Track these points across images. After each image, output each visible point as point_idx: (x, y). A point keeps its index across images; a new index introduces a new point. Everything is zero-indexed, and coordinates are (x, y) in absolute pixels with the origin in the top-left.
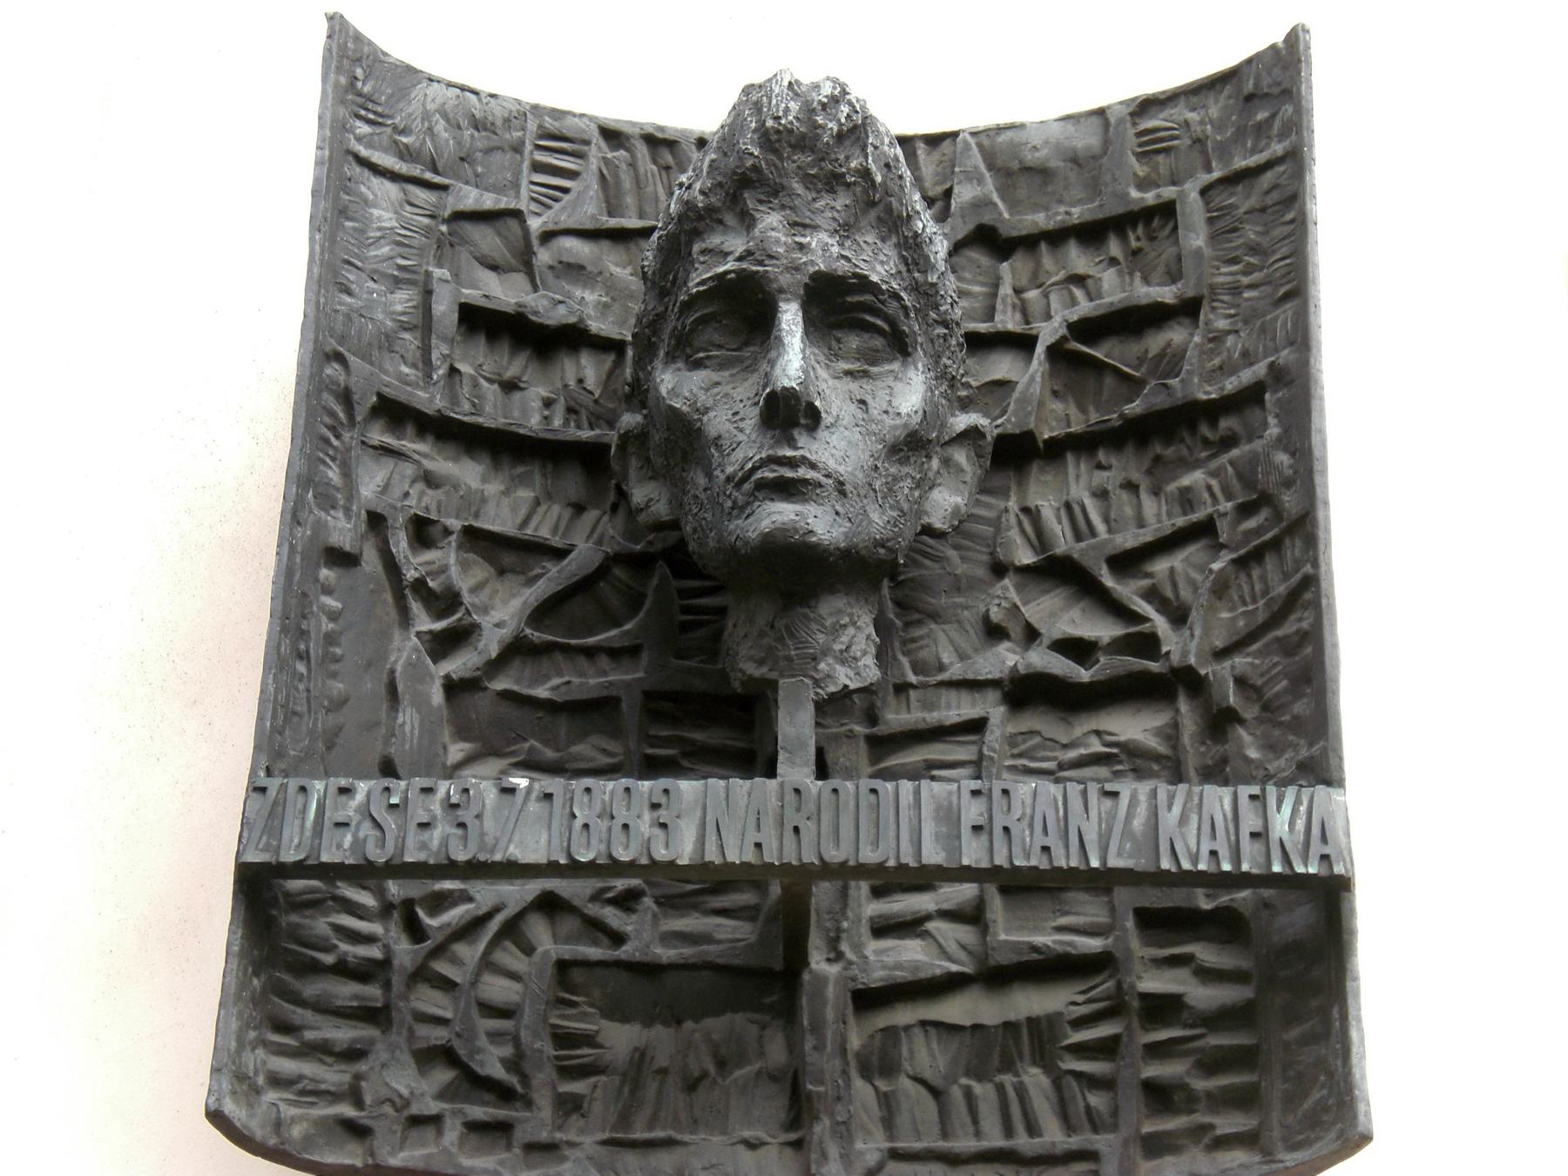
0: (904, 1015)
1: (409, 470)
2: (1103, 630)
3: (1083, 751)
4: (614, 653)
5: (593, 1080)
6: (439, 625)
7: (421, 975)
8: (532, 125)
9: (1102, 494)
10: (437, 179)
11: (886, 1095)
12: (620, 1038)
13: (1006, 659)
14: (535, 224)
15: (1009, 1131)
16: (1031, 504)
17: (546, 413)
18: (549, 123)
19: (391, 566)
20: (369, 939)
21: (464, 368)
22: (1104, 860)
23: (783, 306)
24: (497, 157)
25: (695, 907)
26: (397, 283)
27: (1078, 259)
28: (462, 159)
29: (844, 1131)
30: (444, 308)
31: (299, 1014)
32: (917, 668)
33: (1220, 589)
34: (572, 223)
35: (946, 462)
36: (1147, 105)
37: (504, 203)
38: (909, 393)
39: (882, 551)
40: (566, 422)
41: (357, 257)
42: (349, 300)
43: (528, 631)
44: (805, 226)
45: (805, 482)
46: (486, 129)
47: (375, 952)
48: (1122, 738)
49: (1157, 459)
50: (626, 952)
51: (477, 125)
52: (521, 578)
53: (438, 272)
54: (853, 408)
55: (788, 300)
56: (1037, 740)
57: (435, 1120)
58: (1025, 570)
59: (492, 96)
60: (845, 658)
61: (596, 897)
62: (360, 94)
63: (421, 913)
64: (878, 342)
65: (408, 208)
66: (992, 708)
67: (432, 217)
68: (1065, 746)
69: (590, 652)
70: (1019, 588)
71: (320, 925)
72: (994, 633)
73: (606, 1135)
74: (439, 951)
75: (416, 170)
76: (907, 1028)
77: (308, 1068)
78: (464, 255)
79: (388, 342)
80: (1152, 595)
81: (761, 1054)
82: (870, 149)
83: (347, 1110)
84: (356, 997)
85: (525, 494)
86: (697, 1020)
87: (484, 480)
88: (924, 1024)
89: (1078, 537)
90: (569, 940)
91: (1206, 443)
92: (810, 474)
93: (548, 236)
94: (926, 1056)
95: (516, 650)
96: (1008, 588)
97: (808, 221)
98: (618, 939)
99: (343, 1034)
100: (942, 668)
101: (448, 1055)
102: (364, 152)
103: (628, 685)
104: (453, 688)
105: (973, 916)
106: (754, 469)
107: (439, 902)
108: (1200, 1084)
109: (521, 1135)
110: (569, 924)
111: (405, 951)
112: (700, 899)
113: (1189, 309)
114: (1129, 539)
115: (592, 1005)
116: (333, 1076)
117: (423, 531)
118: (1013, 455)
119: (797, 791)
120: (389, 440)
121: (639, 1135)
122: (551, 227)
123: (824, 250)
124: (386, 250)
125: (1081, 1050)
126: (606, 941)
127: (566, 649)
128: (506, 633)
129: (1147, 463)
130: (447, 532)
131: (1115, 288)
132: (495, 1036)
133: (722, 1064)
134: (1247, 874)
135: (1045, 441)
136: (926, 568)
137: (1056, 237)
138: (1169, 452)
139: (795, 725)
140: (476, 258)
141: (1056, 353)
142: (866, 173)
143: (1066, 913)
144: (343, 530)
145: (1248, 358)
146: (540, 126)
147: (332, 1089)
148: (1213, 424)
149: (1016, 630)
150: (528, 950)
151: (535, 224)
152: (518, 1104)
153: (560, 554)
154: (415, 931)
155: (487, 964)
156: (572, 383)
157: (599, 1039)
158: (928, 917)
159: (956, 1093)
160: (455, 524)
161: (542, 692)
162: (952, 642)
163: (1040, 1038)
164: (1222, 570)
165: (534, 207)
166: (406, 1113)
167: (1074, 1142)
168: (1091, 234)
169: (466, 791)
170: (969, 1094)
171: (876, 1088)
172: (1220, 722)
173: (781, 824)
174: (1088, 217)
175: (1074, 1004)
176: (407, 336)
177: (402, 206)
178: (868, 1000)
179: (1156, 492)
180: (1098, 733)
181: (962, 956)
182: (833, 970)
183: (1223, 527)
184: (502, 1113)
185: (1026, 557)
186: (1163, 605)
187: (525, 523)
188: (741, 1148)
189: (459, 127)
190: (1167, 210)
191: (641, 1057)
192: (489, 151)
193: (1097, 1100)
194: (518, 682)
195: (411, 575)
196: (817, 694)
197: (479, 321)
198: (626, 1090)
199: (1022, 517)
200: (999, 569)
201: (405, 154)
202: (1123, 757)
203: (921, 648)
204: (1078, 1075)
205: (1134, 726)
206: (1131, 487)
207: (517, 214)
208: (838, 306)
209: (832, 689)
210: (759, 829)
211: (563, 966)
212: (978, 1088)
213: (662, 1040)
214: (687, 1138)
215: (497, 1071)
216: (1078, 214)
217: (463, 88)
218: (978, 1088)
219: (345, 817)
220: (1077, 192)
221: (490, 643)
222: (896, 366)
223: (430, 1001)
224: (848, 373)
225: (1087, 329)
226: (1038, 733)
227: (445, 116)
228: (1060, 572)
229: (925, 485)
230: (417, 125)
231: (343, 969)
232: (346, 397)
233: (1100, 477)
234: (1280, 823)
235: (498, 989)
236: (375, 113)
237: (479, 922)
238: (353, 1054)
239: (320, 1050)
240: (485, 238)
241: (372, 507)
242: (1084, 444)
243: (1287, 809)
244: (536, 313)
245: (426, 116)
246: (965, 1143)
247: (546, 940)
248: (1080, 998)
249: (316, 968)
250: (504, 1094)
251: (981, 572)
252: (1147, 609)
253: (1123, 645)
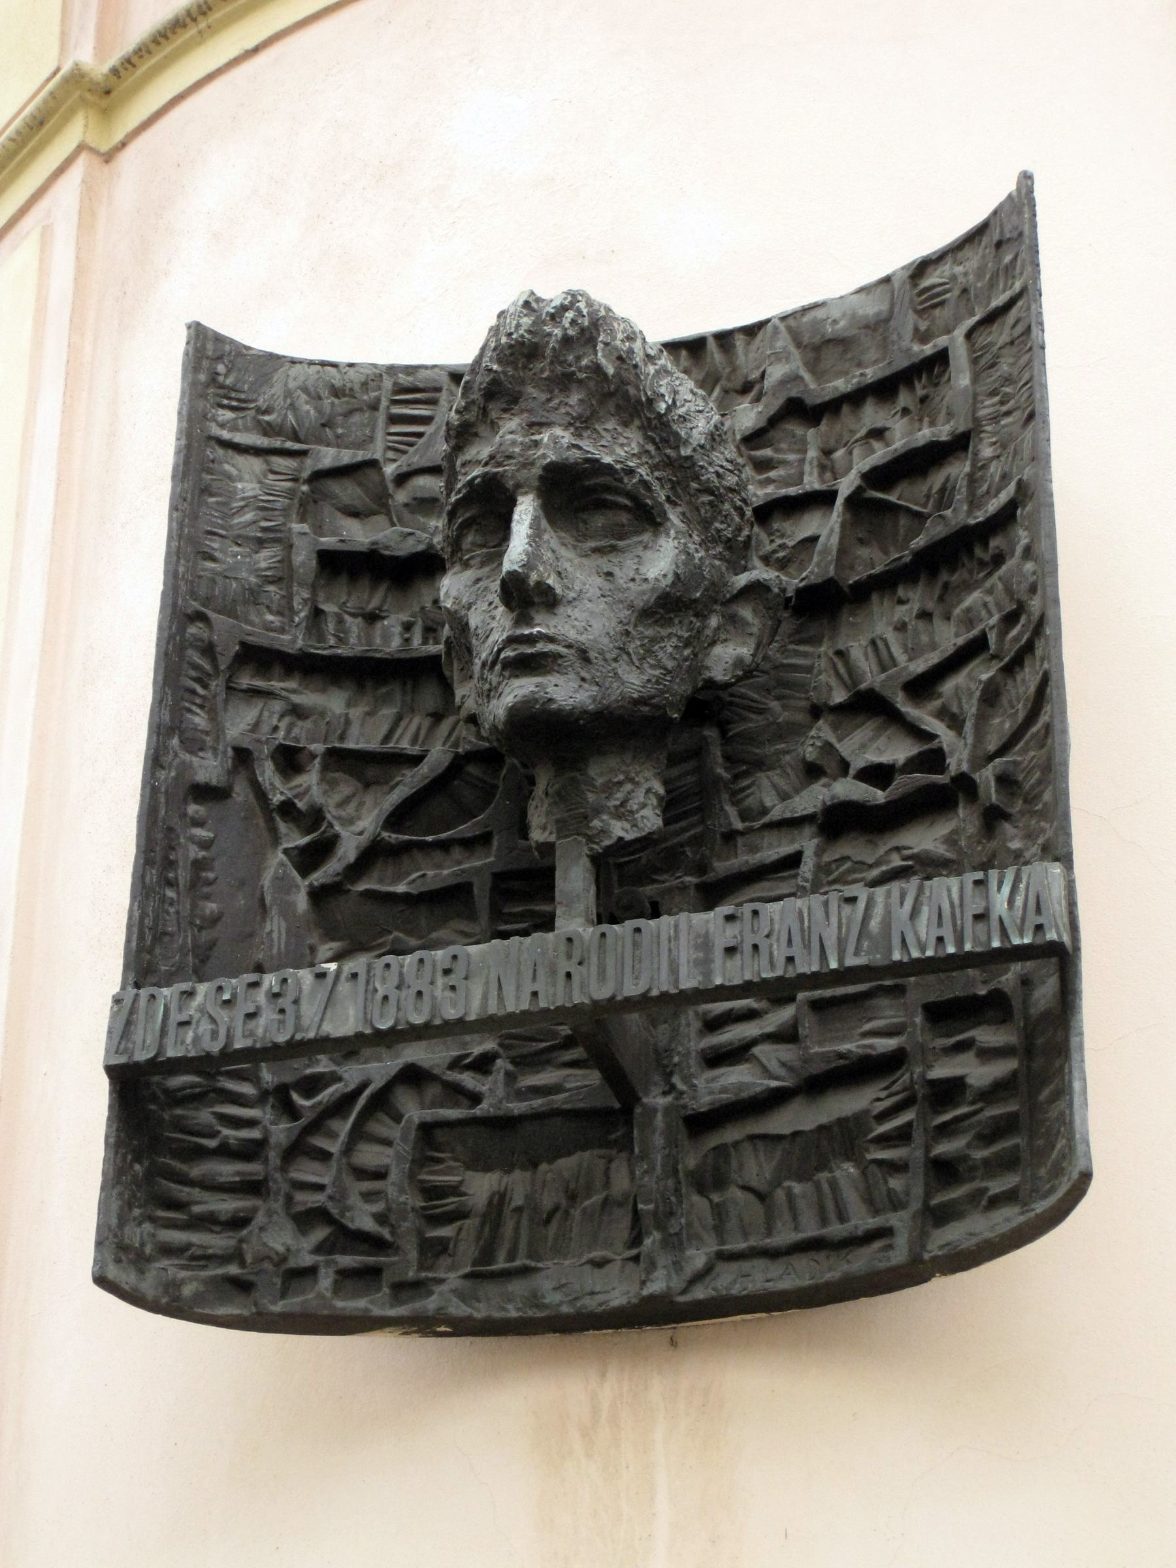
0: (731, 1134)
1: (277, 706)
3: (884, 868)
4: (468, 844)
5: (459, 1223)
6: (304, 840)
7: (296, 1150)
8: (388, 384)
9: (901, 627)
10: (297, 446)
11: (717, 1205)
12: (481, 1187)
14: (389, 470)
15: (824, 1221)
16: (841, 646)
17: (407, 636)
18: (403, 379)
19: (261, 795)
20: (251, 1123)
21: (329, 608)
22: (841, 960)
23: (520, 499)
24: (356, 418)
25: (548, 1062)
26: (260, 543)
27: (872, 415)
28: (324, 425)
30: (303, 558)
31: (183, 1192)
32: (744, 816)
34: (425, 463)
35: (733, 620)
36: (922, 267)
37: (361, 456)
38: (660, 560)
39: (646, 709)
40: (425, 642)
41: (222, 527)
42: (210, 565)
43: (385, 834)
44: (541, 425)
45: (544, 655)
46: (344, 395)
47: (255, 1134)
48: (916, 851)
49: (946, 586)
50: (484, 1108)
51: (336, 392)
52: (386, 788)
53: (297, 527)
54: (599, 581)
55: (526, 493)
56: (848, 865)
57: (310, 1272)
58: (840, 709)
59: (351, 365)
60: (622, 812)
61: (456, 1064)
62: (222, 387)
63: (295, 1096)
64: (624, 518)
65: (271, 476)
66: (807, 843)
67: (295, 480)
68: (871, 866)
69: (444, 846)
70: (835, 727)
71: (204, 1116)
72: (813, 772)
73: (468, 1270)
74: (316, 1126)
75: (277, 443)
76: (736, 1144)
77: (196, 1238)
78: (327, 510)
79: (253, 596)
80: (943, 714)
81: (607, 1184)
82: (600, 346)
83: (233, 1270)
84: (238, 1173)
85: (388, 712)
86: (551, 1161)
87: (349, 705)
88: (752, 1138)
89: (884, 669)
90: (433, 1105)
91: (982, 564)
92: (551, 647)
93: (402, 479)
94: (756, 1168)
95: (373, 854)
96: (823, 730)
97: (544, 420)
98: (475, 1098)
99: (227, 1205)
100: (765, 811)
101: (320, 1215)
102: (225, 435)
103: (478, 871)
104: (318, 896)
105: (787, 1036)
106: (500, 651)
107: (311, 1085)
108: (979, 1154)
109: (388, 1277)
110: (433, 1091)
111: (281, 1131)
112: (555, 1054)
114: (919, 666)
115: (456, 1160)
116: (217, 1242)
117: (290, 760)
118: (822, 605)
119: (570, 940)
120: (259, 683)
121: (501, 1264)
122: (405, 469)
123: (557, 442)
124: (249, 516)
125: (884, 1140)
126: (465, 1102)
127: (422, 846)
128: (364, 840)
129: (937, 592)
130: (313, 756)
131: (905, 434)
132: (368, 1197)
133: (573, 1197)
134: (970, 954)
135: (851, 587)
136: (751, 720)
137: (856, 398)
138: (955, 578)
139: (575, 880)
140: (339, 510)
141: (855, 502)
142: (597, 369)
143: (870, 1020)
144: (209, 768)
146: (395, 384)
147: (219, 1252)
148: (986, 545)
149: (831, 766)
150: (397, 1118)
151: (389, 470)
152: (390, 1251)
153: (417, 760)
154: (292, 1112)
155: (358, 1134)
156: (428, 605)
157: (463, 1189)
158: (754, 1042)
159: (780, 1194)
160: (318, 748)
161: (401, 888)
162: (774, 786)
163: (846, 1137)
164: (991, 679)
165: (391, 455)
166: (284, 1267)
167: (872, 1223)
169: (285, 980)
170: (790, 1196)
171: (710, 1201)
173: (553, 972)
174: (880, 375)
175: (879, 1100)
176: (271, 588)
177: (265, 476)
178: (700, 1123)
180: (897, 849)
181: (782, 1072)
182: (662, 1101)
183: (992, 638)
184: (371, 1260)
185: (839, 696)
187: (387, 738)
188: (588, 1267)
189: (320, 398)
190: (941, 358)
191: (499, 1201)
192: (349, 413)
194: (381, 881)
195: (277, 799)
196: (591, 849)
197: (336, 565)
198: (487, 1229)
199: (836, 660)
200: (816, 712)
201: (268, 430)
202: (917, 867)
203: (748, 796)
204: (880, 1163)
205: (925, 838)
207: (373, 464)
208: (575, 495)
209: (607, 843)
210: (534, 978)
211: (427, 1130)
213: (518, 1183)
214: (540, 1265)
215: (366, 1223)
216: (871, 374)
217: (323, 364)
218: (797, 1188)
219: (204, 1017)
220: (872, 355)
221: (348, 849)
222: (646, 537)
223: (308, 1172)
224: (595, 550)
226: (847, 858)
227: (305, 390)
228: (868, 706)
229: (699, 644)
230: (279, 403)
231: (226, 1152)
232: (209, 650)
233: (901, 612)
234: (1000, 901)
235: (369, 1155)
236: (238, 400)
237: (349, 1099)
238: (238, 1222)
239: (207, 1222)
240: (347, 491)
241: (235, 743)
242: (886, 583)
243: (1006, 889)
244: (387, 548)
245: (288, 394)
247: (414, 1110)
248: (883, 1094)
249: (201, 1153)
250: (376, 1244)
251: (800, 717)
253: (912, 765)
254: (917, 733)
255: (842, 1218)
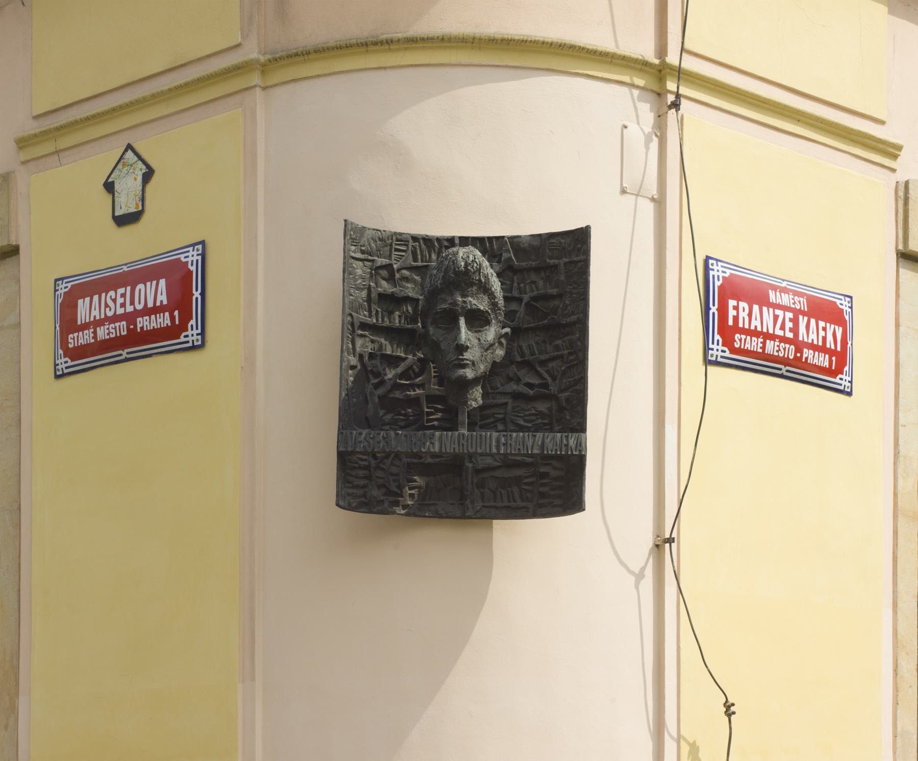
0: (486, 475)
2: (536, 381)
9: (537, 343)
13: (513, 387)
15: (509, 501)
27: (533, 277)
29: (472, 502)
33: (564, 373)
80: (548, 372)
101: (384, 486)
109: (401, 503)
113: (560, 296)
114: (543, 357)
145: (573, 314)
168: (537, 270)
172: (561, 409)
178: (478, 471)
179: (550, 344)
186: (550, 375)
190: (556, 266)
193: (529, 495)
195: (369, 369)
206: (544, 342)
212: (503, 491)
218: (503, 491)
225: (534, 299)
246: (500, 504)
252: (546, 375)
254: (540, 376)
255: (515, 501)
